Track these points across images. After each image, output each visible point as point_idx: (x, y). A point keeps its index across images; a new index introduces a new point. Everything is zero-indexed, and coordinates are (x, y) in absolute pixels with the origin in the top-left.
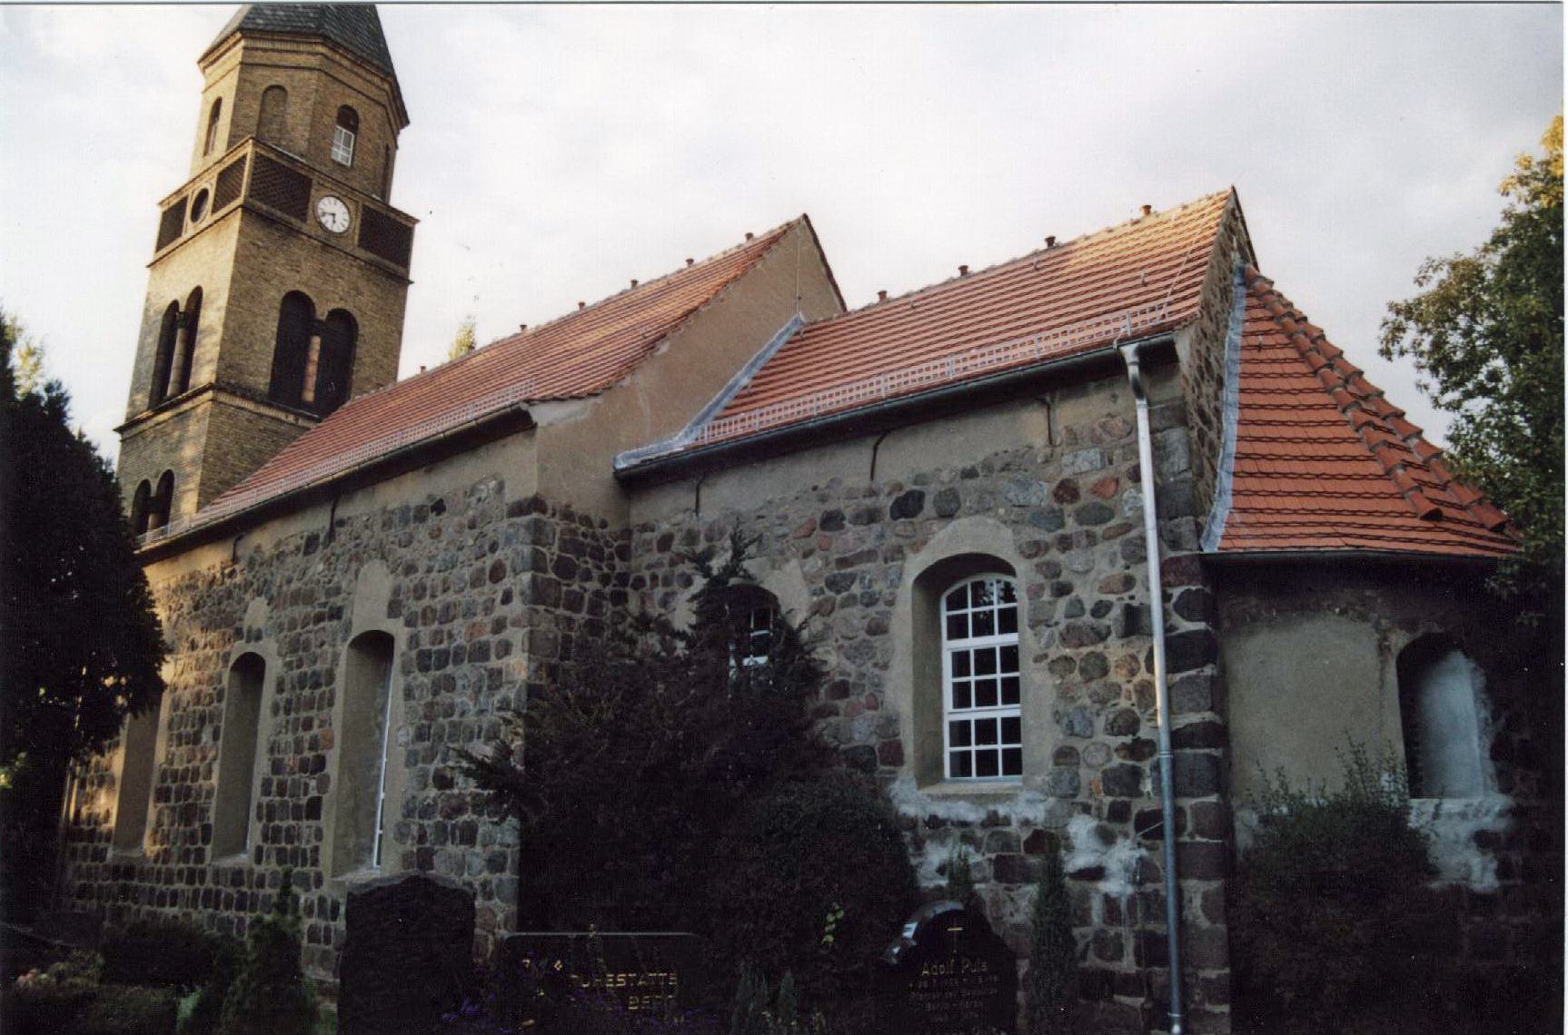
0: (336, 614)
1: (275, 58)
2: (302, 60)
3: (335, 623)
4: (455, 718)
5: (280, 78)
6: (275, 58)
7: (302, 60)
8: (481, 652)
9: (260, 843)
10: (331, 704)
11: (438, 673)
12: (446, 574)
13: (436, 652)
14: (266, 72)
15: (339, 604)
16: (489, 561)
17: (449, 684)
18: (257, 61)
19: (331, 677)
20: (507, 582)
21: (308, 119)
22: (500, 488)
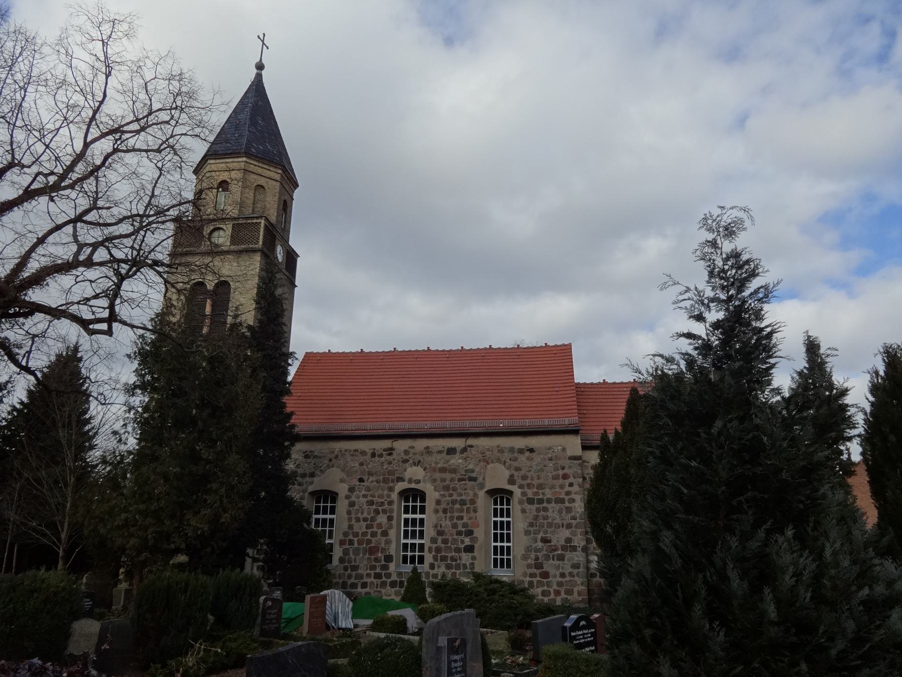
0: (474, 479)
1: (260, 171)
2: (272, 174)
3: (472, 482)
4: (550, 520)
5: (262, 181)
6: (260, 171)
7: (272, 174)
8: (562, 501)
9: (432, 561)
10: (475, 511)
11: (539, 506)
12: (539, 474)
13: (537, 499)
14: (256, 177)
15: (475, 476)
16: (561, 472)
17: (545, 509)
18: (251, 170)
19: (473, 502)
20: (571, 480)
21: (276, 206)
22: (564, 449)
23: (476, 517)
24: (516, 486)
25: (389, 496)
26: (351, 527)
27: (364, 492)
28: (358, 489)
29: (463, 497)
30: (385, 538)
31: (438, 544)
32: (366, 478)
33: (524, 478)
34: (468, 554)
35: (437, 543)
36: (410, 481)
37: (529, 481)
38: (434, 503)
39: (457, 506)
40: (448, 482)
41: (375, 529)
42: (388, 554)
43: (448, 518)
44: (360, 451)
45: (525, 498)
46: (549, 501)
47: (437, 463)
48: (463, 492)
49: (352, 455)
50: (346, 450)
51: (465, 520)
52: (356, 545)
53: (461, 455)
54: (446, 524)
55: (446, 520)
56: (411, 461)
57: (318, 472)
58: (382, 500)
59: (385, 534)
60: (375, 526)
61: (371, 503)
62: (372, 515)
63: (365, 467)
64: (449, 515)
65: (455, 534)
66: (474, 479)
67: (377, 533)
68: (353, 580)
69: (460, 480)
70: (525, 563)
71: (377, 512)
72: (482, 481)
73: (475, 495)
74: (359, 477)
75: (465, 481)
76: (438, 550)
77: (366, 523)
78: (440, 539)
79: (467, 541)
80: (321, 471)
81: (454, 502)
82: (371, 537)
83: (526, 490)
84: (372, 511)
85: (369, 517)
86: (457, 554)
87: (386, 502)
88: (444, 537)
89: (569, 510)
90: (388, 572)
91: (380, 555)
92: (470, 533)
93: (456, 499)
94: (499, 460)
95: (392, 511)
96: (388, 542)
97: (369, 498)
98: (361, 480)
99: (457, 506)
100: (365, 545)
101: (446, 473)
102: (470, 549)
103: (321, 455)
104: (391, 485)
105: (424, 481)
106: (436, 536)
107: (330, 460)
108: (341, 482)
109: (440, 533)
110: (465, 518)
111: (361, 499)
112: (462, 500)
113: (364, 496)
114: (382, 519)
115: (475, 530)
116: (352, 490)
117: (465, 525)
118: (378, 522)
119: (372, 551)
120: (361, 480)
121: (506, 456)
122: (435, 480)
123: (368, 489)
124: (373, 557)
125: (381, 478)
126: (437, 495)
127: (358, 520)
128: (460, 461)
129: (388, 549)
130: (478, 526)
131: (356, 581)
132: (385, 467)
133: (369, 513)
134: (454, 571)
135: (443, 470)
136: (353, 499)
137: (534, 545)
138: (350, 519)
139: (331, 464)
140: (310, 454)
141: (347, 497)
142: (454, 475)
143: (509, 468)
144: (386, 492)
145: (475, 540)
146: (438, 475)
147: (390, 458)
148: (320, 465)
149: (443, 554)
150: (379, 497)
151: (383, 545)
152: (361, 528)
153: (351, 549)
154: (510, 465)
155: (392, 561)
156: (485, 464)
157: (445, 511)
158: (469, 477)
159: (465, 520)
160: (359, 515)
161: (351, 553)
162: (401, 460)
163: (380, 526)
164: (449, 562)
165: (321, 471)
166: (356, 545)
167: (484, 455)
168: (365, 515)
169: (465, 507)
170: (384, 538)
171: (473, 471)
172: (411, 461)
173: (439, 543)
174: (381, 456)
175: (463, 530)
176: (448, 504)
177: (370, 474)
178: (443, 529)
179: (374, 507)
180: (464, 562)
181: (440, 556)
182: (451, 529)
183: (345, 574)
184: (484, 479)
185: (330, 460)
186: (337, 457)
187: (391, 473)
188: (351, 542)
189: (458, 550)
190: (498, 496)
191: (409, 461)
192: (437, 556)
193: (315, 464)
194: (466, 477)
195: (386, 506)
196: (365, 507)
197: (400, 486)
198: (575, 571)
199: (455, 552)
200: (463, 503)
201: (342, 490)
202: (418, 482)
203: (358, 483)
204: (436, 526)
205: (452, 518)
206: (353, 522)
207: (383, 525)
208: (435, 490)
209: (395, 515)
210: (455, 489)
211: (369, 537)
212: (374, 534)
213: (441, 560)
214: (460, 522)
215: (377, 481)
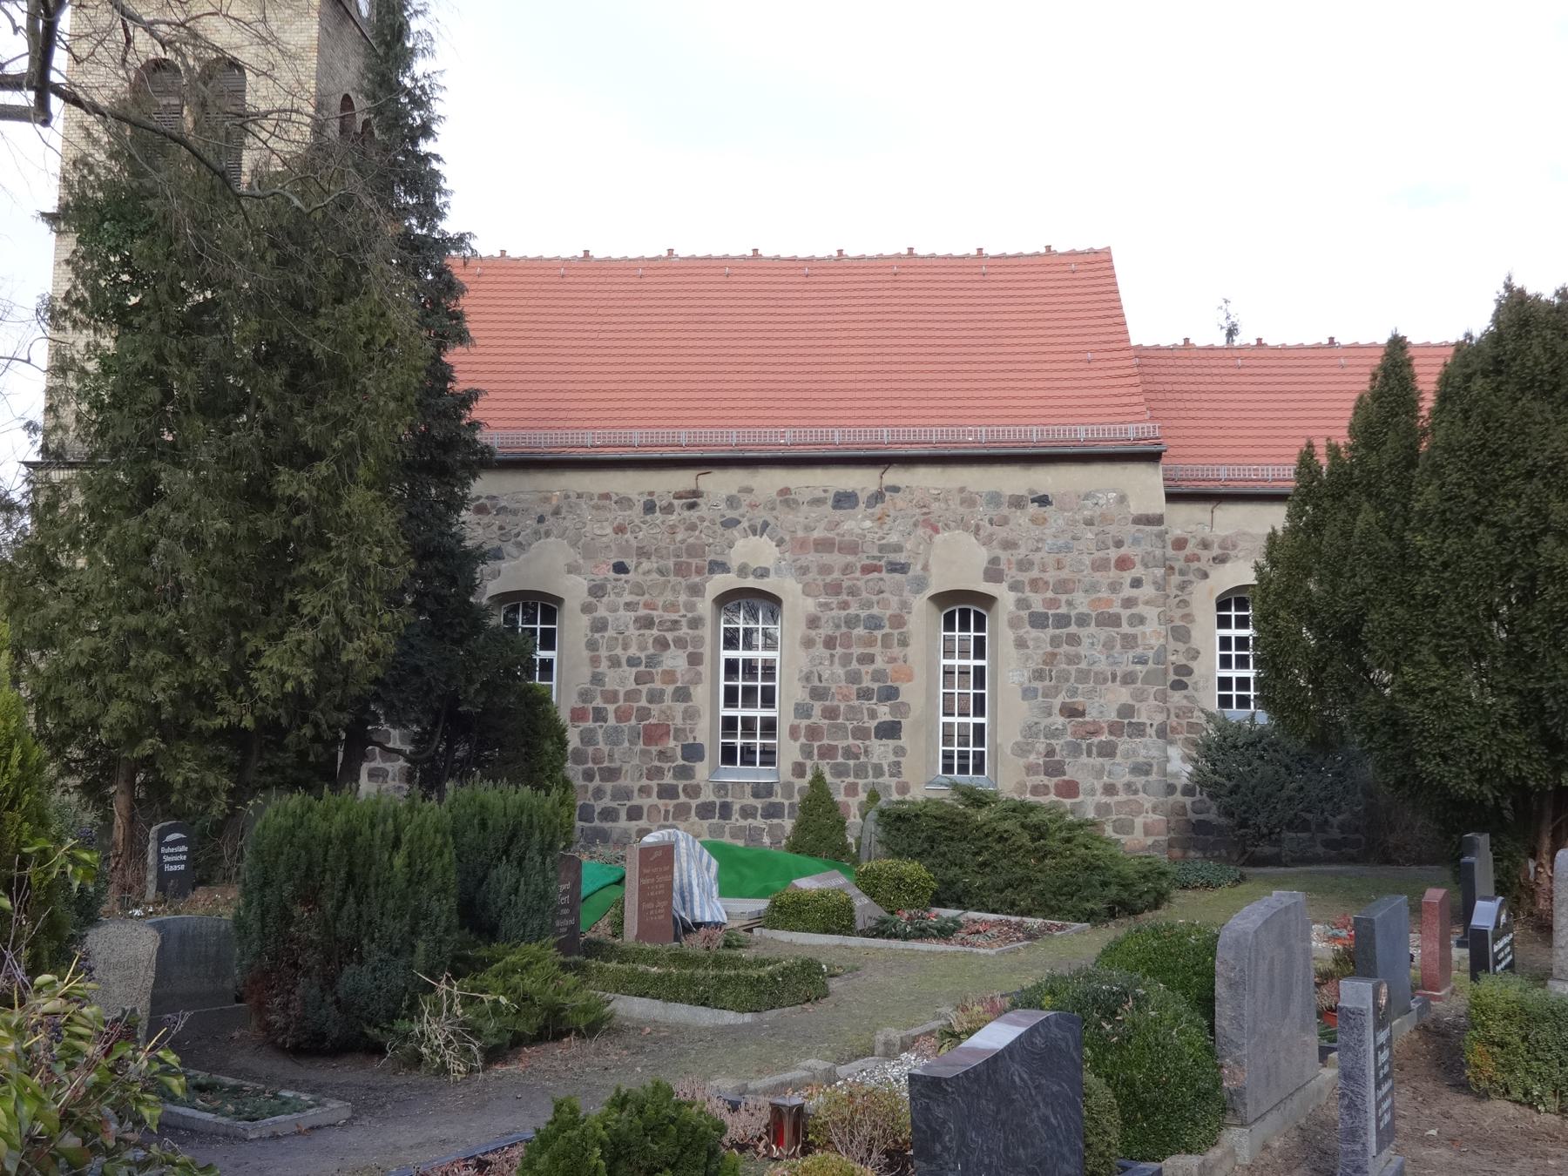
0: (901, 568)
3: (897, 576)
4: (1083, 665)
8: (1115, 621)
9: (800, 759)
10: (904, 643)
11: (1058, 631)
12: (1060, 556)
13: (1055, 615)
16: (1113, 554)
17: (1074, 640)
19: (898, 621)
20: (1138, 571)
22: (1122, 499)
23: (905, 656)
24: (1005, 585)
25: (691, 607)
26: (597, 679)
27: (628, 598)
28: (615, 587)
29: (875, 611)
30: (684, 705)
31: (813, 720)
32: (630, 562)
33: (1025, 565)
34: (885, 741)
35: (809, 716)
36: (743, 571)
37: (1035, 573)
38: (803, 626)
39: (860, 631)
40: (836, 575)
41: (658, 685)
42: (691, 741)
43: (836, 660)
44: (615, 498)
45: (1024, 614)
46: (1082, 620)
47: (808, 528)
48: (875, 598)
49: (597, 508)
50: (579, 496)
51: (879, 663)
52: (612, 721)
53: (870, 511)
54: (833, 673)
55: (832, 662)
56: (745, 524)
57: (509, 548)
58: (674, 617)
59: (683, 695)
60: (657, 678)
61: (648, 623)
62: (651, 651)
63: (628, 535)
64: (839, 651)
65: (854, 696)
66: (901, 568)
67: (662, 692)
68: (606, 802)
69: (867, 570)
70: (1022, 762)
71: (662, 644)
72: (920, 573)
73: (905, 605)
74: (615, 560)
75: (880, 571)
76: (813, 733)
77: (634, 670)
78: (818, 707)
79: (884, 713)
80: (519, 545)
81: (851, 622)
82: (650, 702)
83: (1028, 594)
84: (651, 641)
85: (643, 656)
86: (858, 742)
87: (684, 622)
88: (828, 703)
89: (1129, 641)
90: (694, 782)
91: (672, 743)
92: (890, 694)
93: (858, 615)
94: (963, 524)
95: (698, 641)
96: (691, 715)
97: (642, 612)
98: (620, 568)
99: (860, 631)
100: (633, 722)
101: (832, 552)
102: (890, 730)
103: (517, 506)
104: (697, 579)
105: (778, 571)
106: (808, 700)
107: (541, 519)
108: (569, 572)
109: (818, 694)
110: (879, 659)
111: (622, 612)
112: (872, 617)
113: (628, 605)
114: (675, 660)
115: (904, 688)
116: (597, 591)
117: (878, 676)
118: (665, 668)
119: (653, 734)
120: (620, 568)
121: (982, 512)
122: (804, 570)
123: (639, 589)
124: (654, 749)
125: (671, 563)
126: (810, 605)
127: (615, 662)
128: (868, 524)
129: (692, 731)
130: (910, 678)
131: (614, 804)
132: (679, 537)
133: (643, 648)
134: (851, 779)
135: (824, 545)
136: (602, 612)
137: (1045, 722)
138: (595, 661)
139: (543, 528)
140: (488, 503)
141: (587, 609)
142: (850, 558)
143: (987, 542)
144: (683, 598)
145: (897, 709)
146: (811, 558)
147: (693, 515)
148: (516, 531)
149: (825, 742)
150: (665, 609)
151: (679, 721)
152: (622, 681)
153: (600, 732)
154: (991, 535)
155: (701, 759)
156: (929, 531)
157: (830, 643)
158: (890, 563)
159: (879, 663)
160: (619, 651)
161: (600, 739)
162: (719, 520)
163: (670, 676)
164: (840, 760)
165: (519, 545)
166: (612, 721)
167: (925, 510)
168: (633, 651)
169: (879, 634)
170: (681, 706)
171: (898, 548)
172: (745, 524)
173: (817, 718)
174: (668, 509)
175: (875, 686)
176: (838, 626)
177: (642, 553)
178: (824, 684)
179: (655, 632)
180: (875, 760)
181: (820, 747)
182: (843, 684)
183: (586, 787)
184: (925, 568)
185: (541, 519)
186: (556, 512)
187: (693, 551)
188: (599, 715)
189: (860, 733)
190: (957, 608)
191: (739, 522)
192: (812, 746)
193: (501, 528)
194: (882, 563)
195: (684, 630)
196: (632, 631)
197: (720, 583)
198: (1140, 781)
199: (854, 737)
200: (874, 623)
201: (572, 589)
202: (763, 573)
203: (612, 575)
204: (808, 678)
205: (846, 659)
206: (604, 666)
207: (679, 676)
208: (806, 593)
209: (706, 651)
210: (853, 592)
211: (643, 703)
212: (655, 697)
213: (822, 756)
214: (867, 669)
215: (661, 572)
